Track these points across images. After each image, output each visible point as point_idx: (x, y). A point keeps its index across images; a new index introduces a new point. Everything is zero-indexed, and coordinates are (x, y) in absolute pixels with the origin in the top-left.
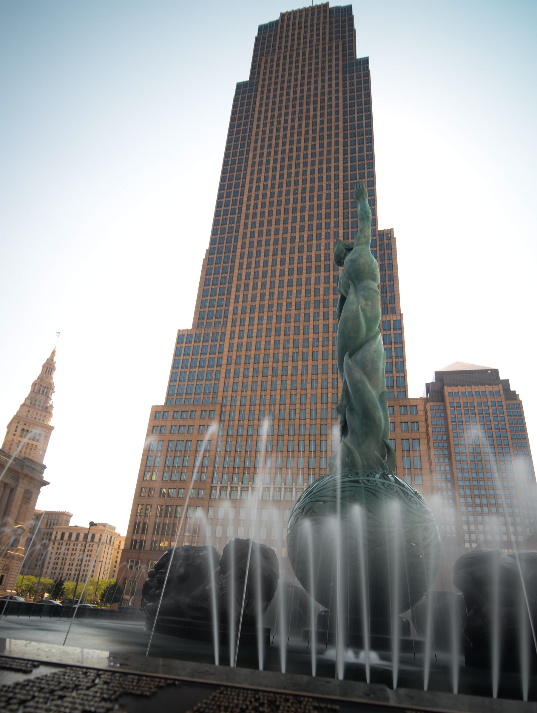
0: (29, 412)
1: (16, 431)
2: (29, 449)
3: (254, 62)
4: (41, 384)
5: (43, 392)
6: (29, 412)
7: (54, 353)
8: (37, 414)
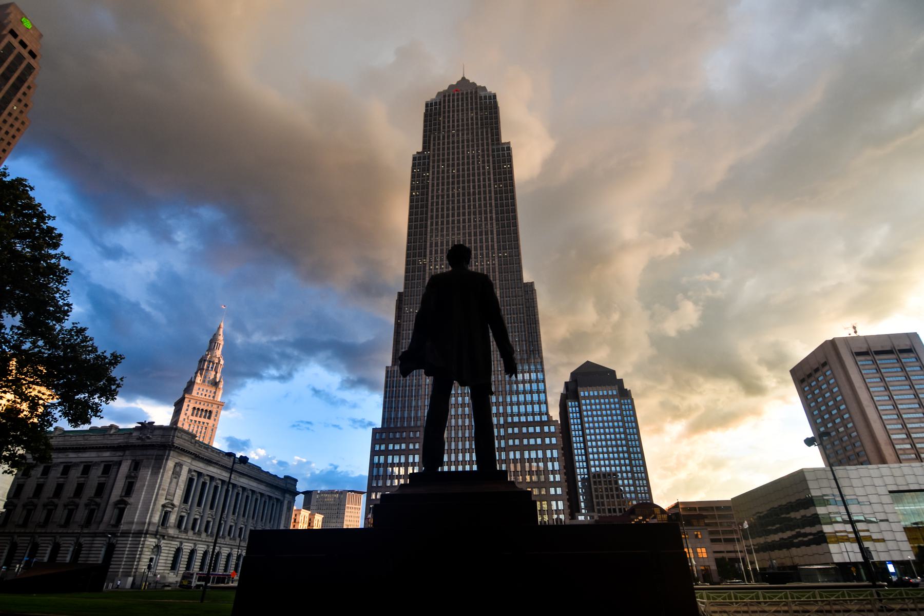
0: (199, 389)
1: (187, 410)
3: (424, 136)
5: (212, 368)
8: (207, 391)
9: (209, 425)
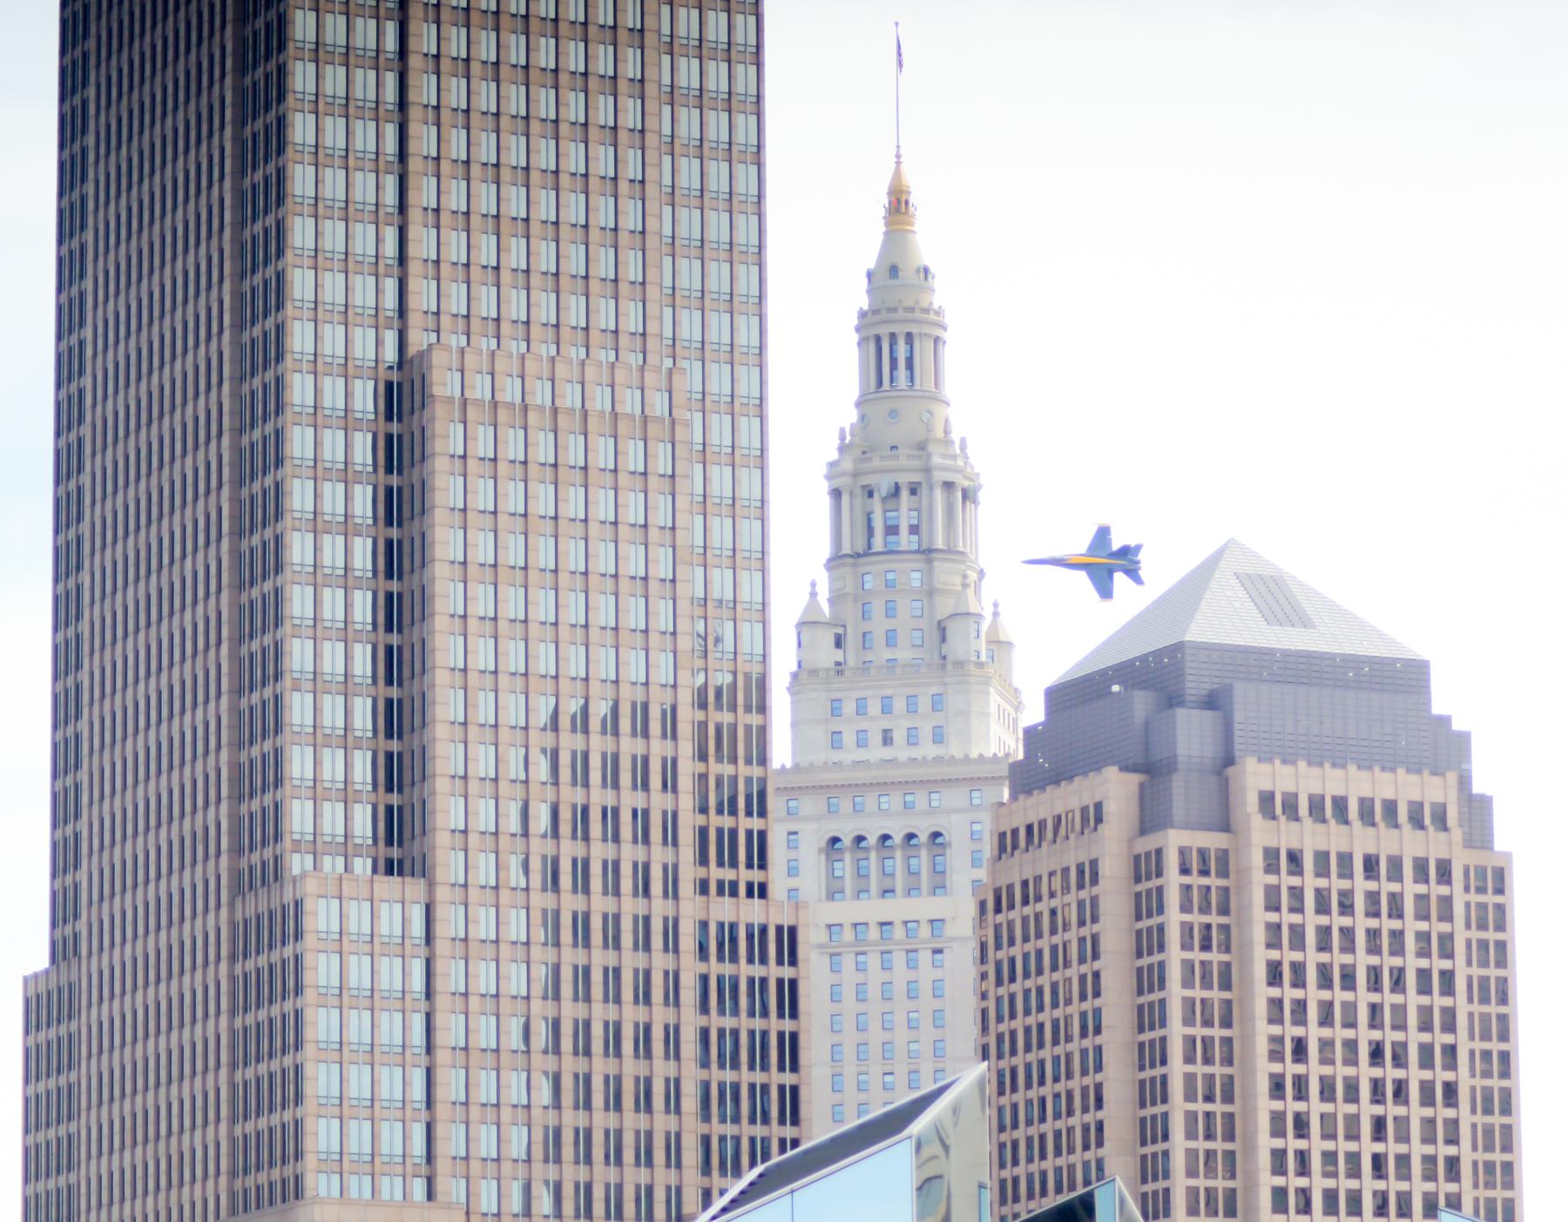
0: (835, 709)
2: (899, 959)
4: (866, 481)
5: (892, 530)
6: (835, 709)
7: (898, 206)
9: (950, 931)
